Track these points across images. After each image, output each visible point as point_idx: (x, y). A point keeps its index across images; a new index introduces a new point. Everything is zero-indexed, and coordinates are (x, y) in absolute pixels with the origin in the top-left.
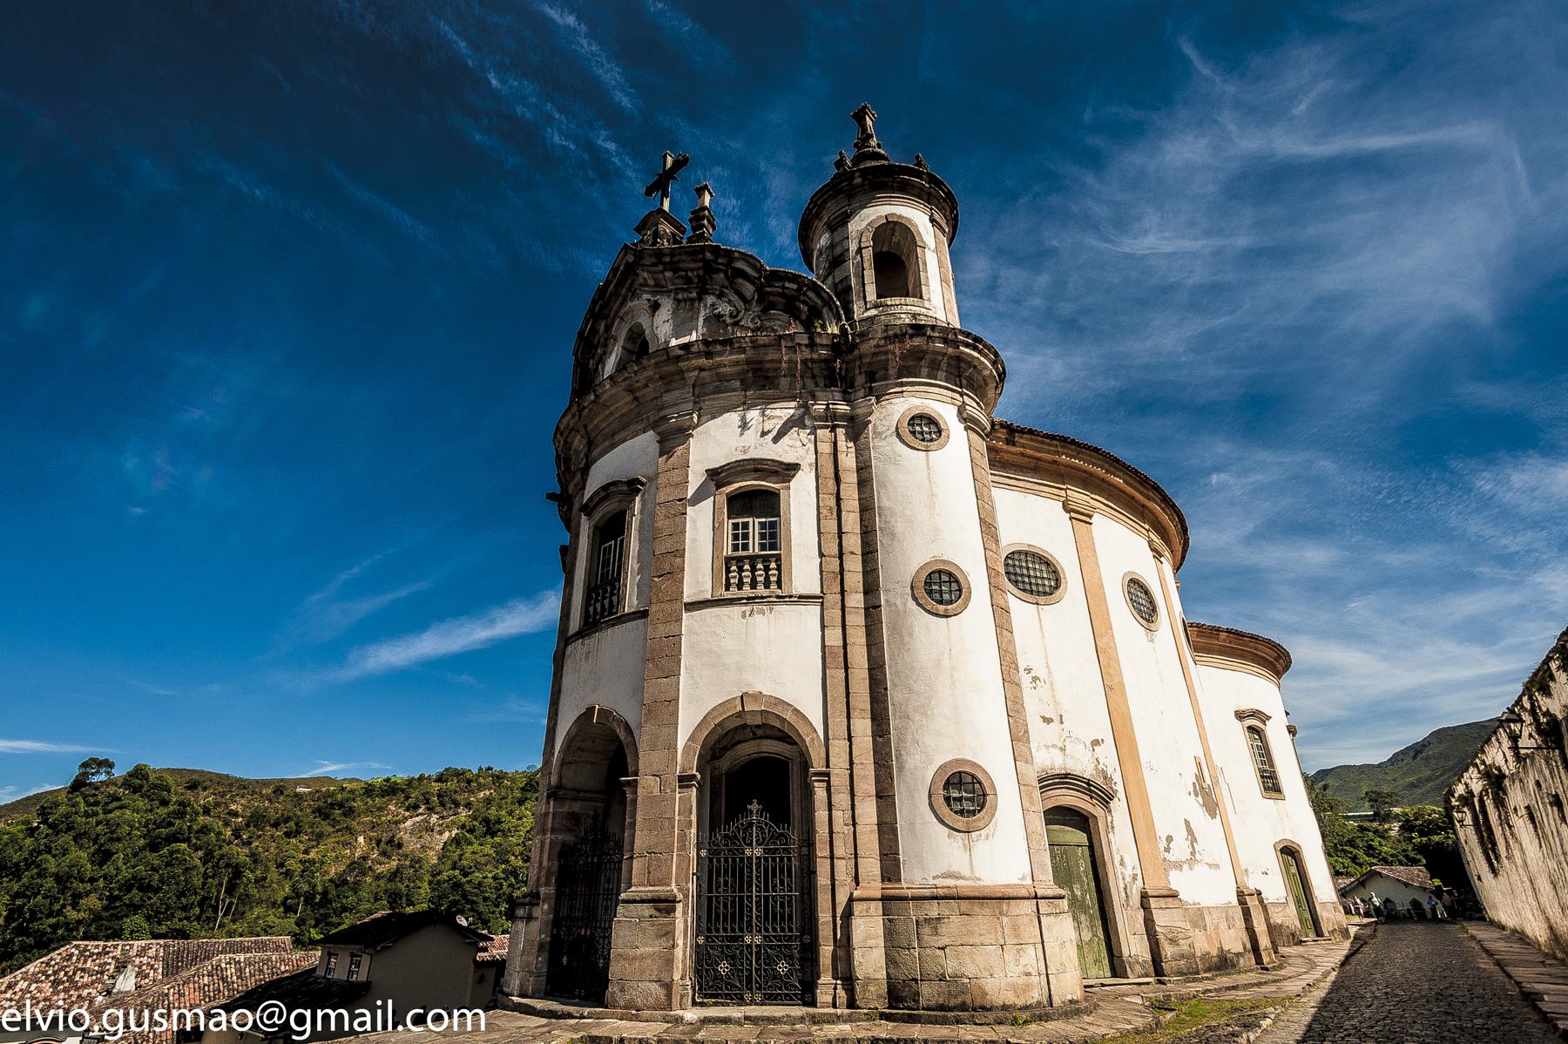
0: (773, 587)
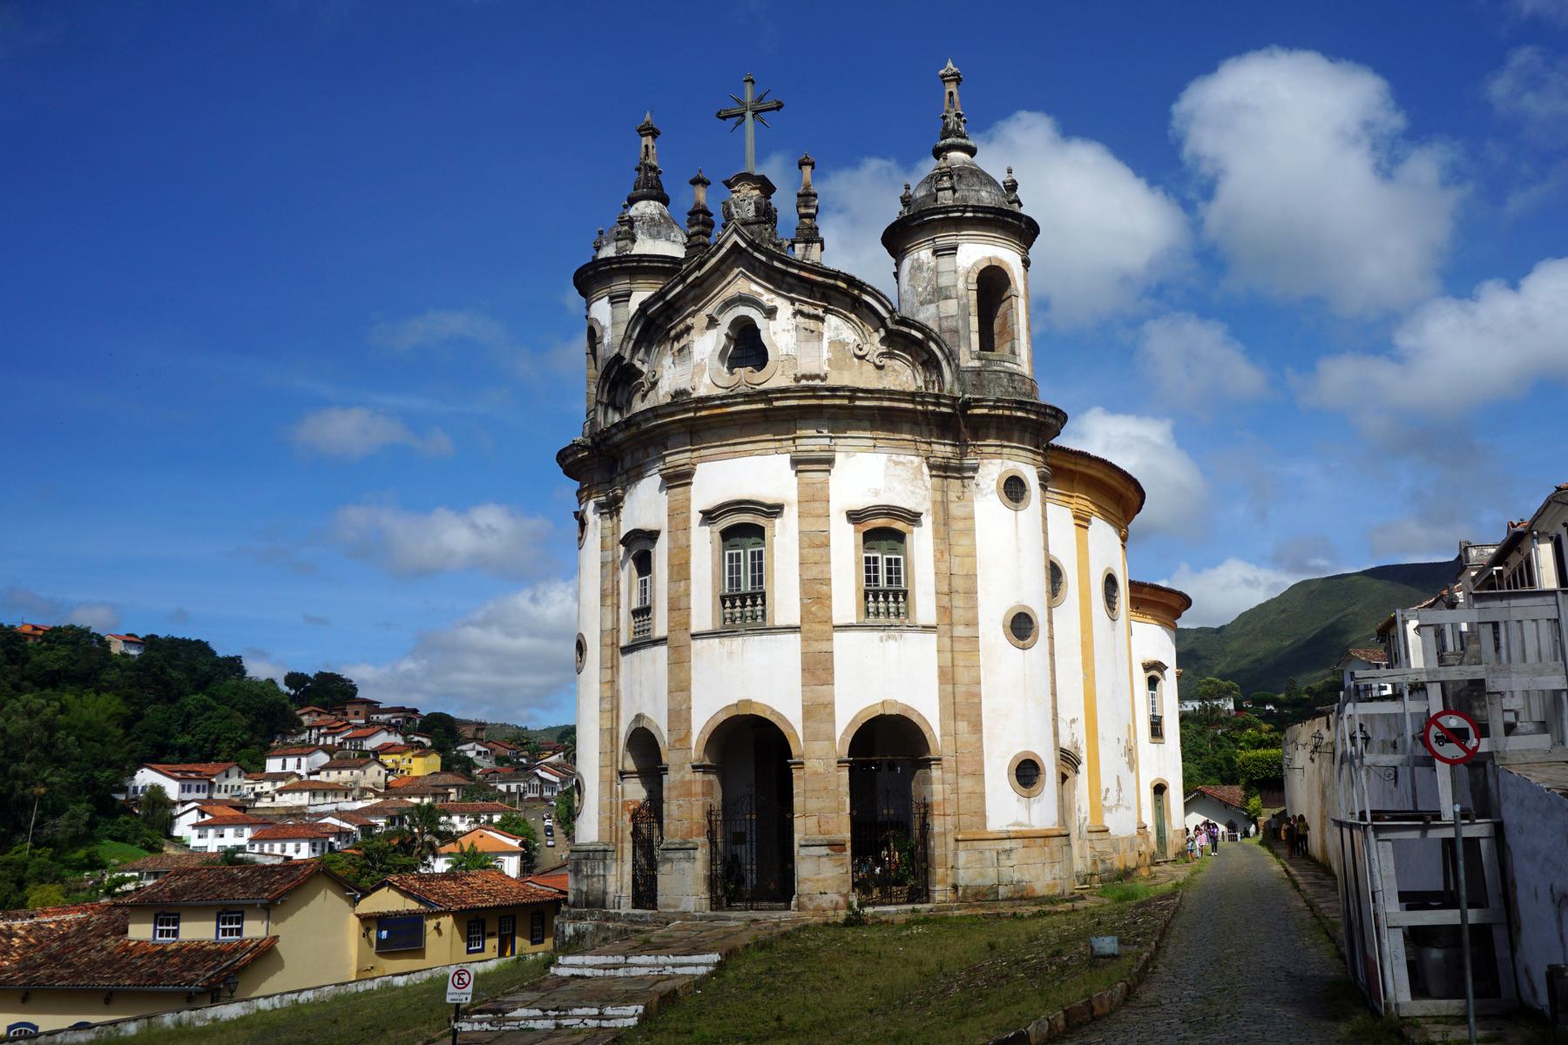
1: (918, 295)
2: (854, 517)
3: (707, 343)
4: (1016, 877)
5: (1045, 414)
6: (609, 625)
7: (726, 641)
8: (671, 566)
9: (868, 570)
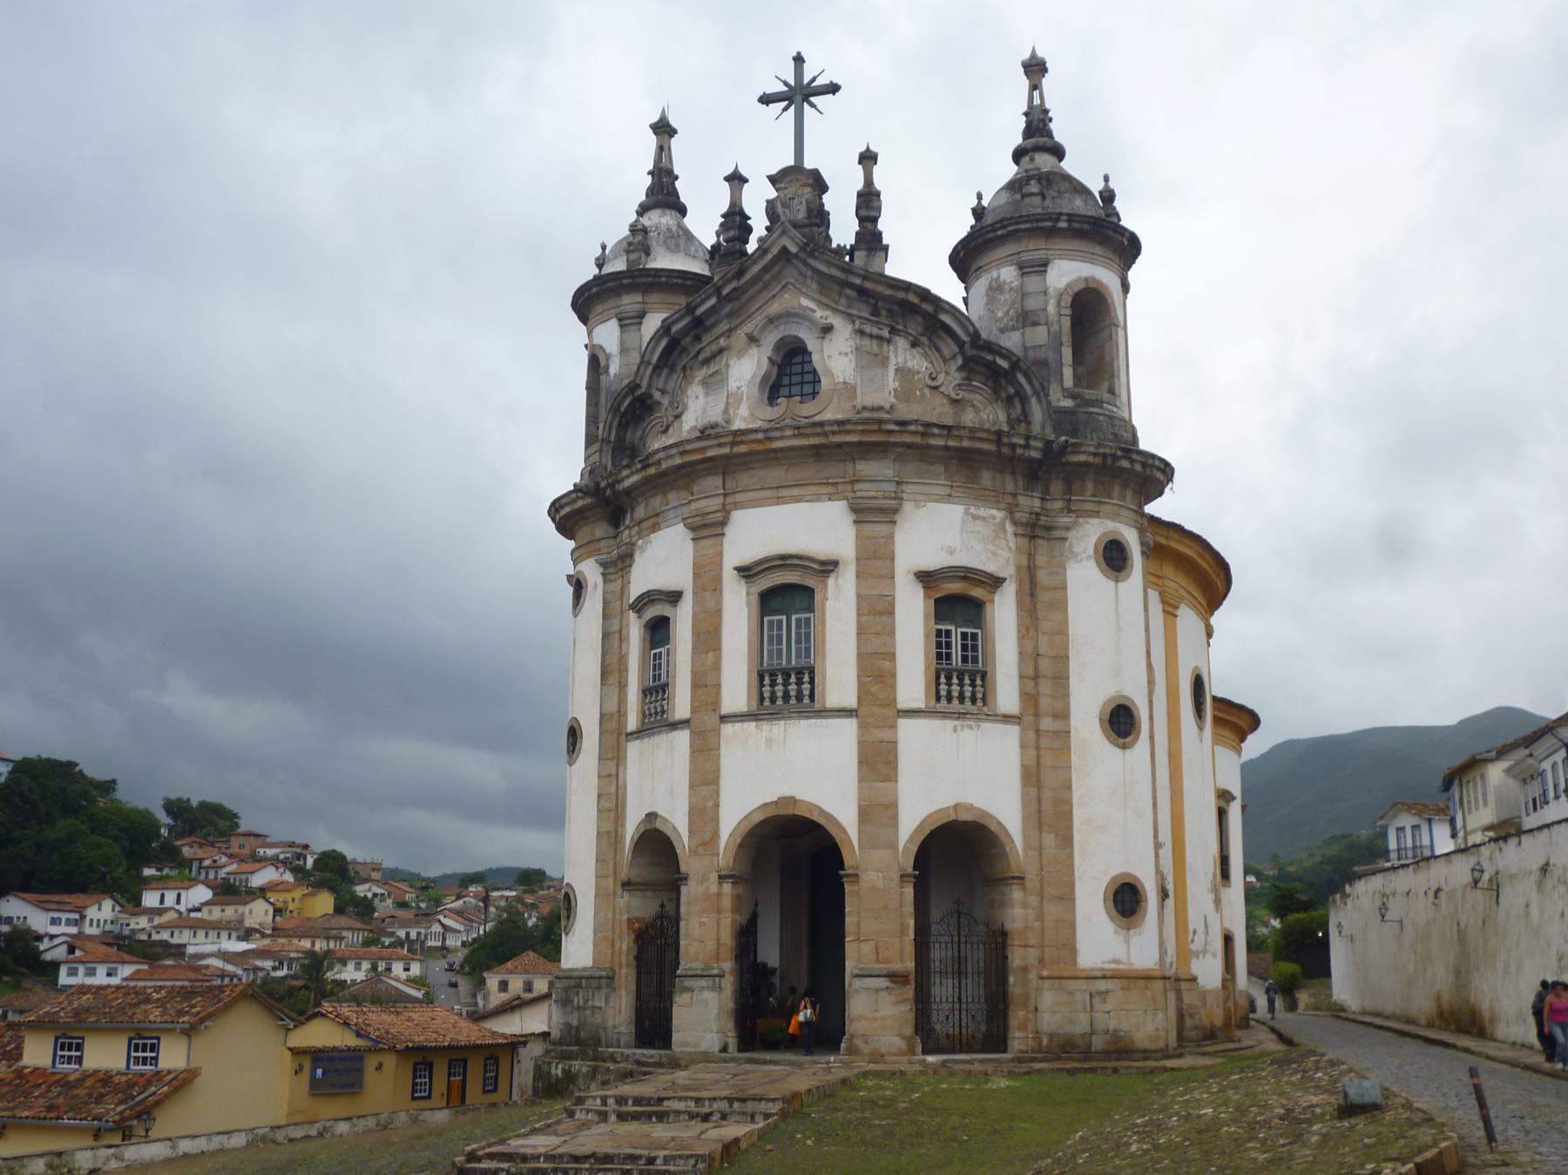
0: (979, 703)
1: (1000, 320)
2: (926, 578)
3: (746, 369)
4: (1112, 1024)
5: (1153, 466)
6: (612, 706)
7: (765, 726)
8: (696, 633)
9: (939, 645)
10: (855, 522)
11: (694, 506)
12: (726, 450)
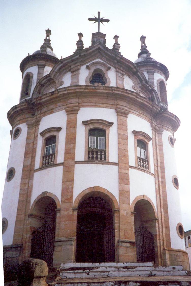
8: (67, 138)
10: (117, 115)
11: (68, 106)
12: (83, 90)
